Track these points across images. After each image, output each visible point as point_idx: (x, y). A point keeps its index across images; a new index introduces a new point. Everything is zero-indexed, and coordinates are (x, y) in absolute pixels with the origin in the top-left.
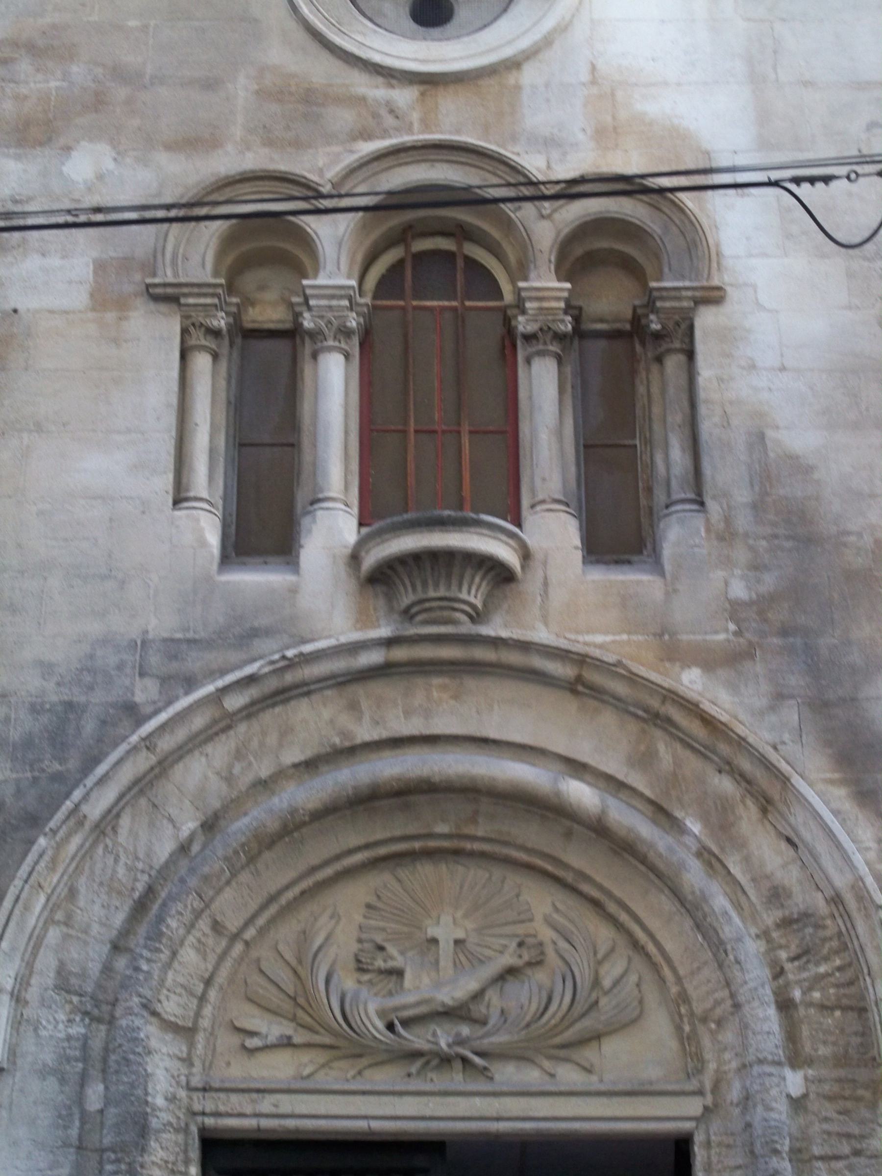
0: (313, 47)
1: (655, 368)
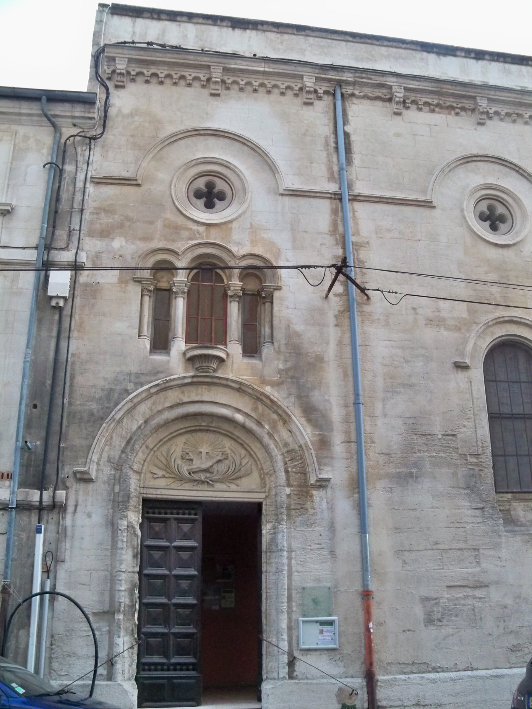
0: (178, 213)
1: (263, 306)
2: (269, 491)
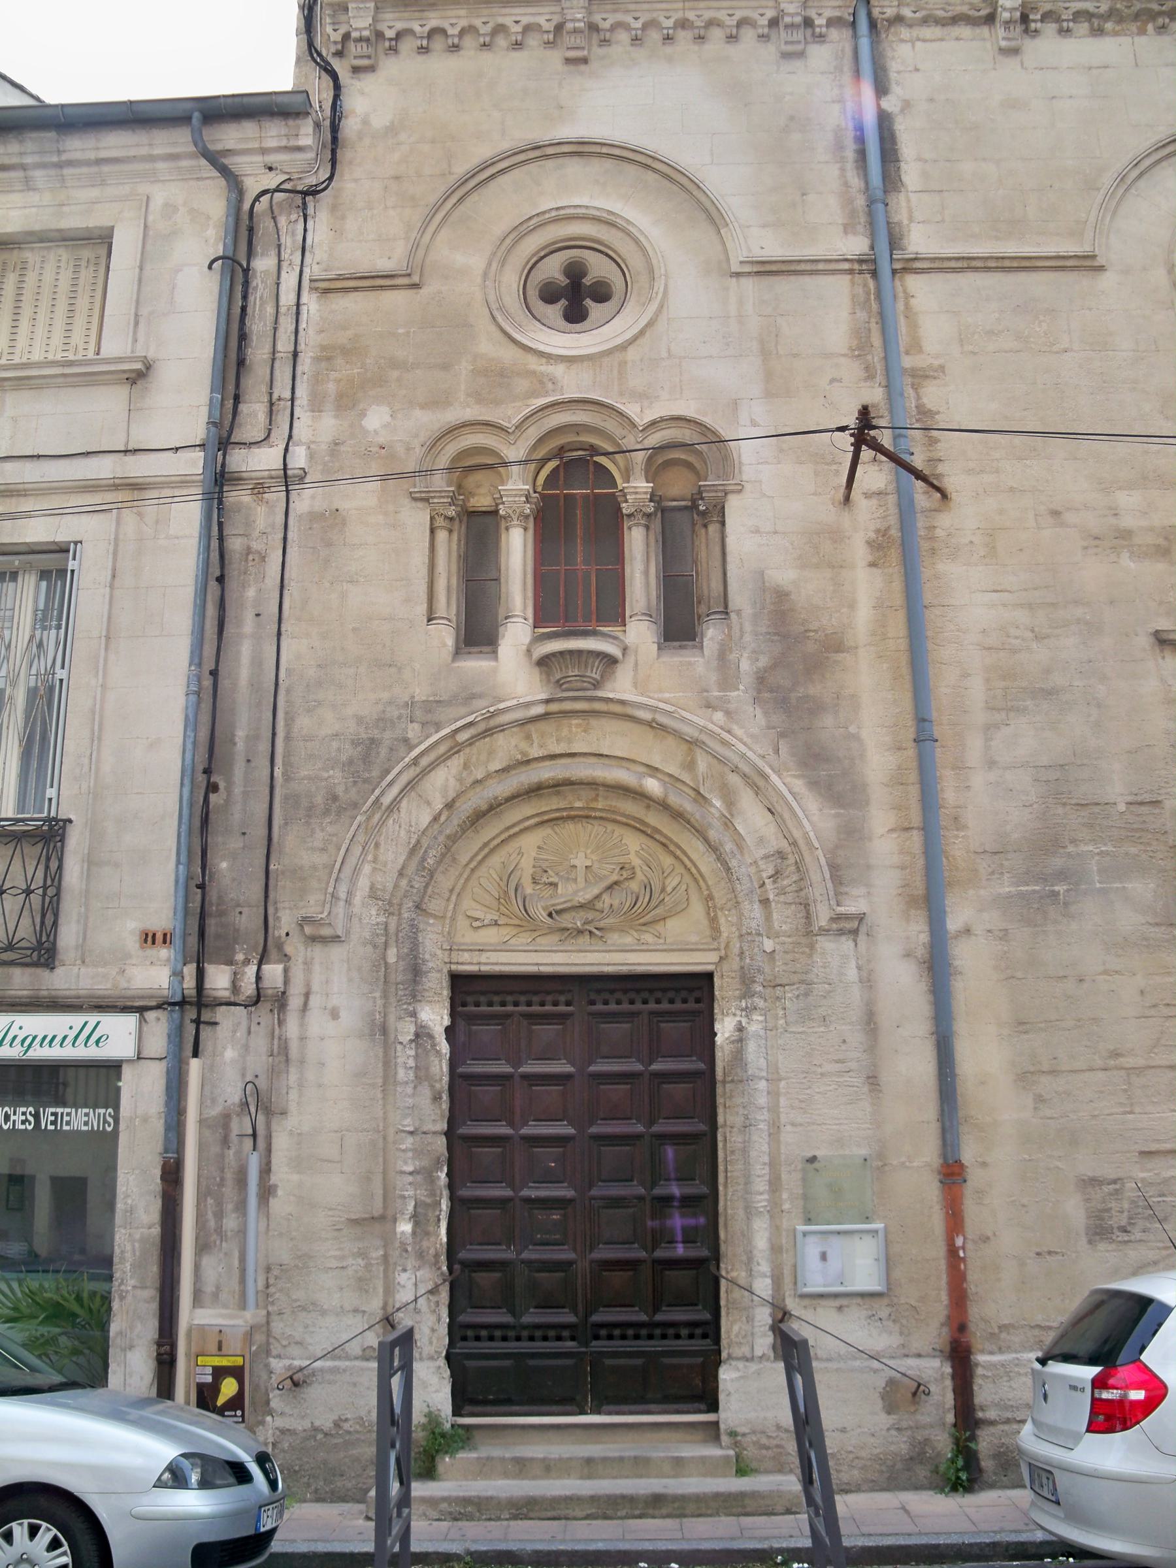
0: (504, 340)
1: (703, 531)
2: (727, 946)
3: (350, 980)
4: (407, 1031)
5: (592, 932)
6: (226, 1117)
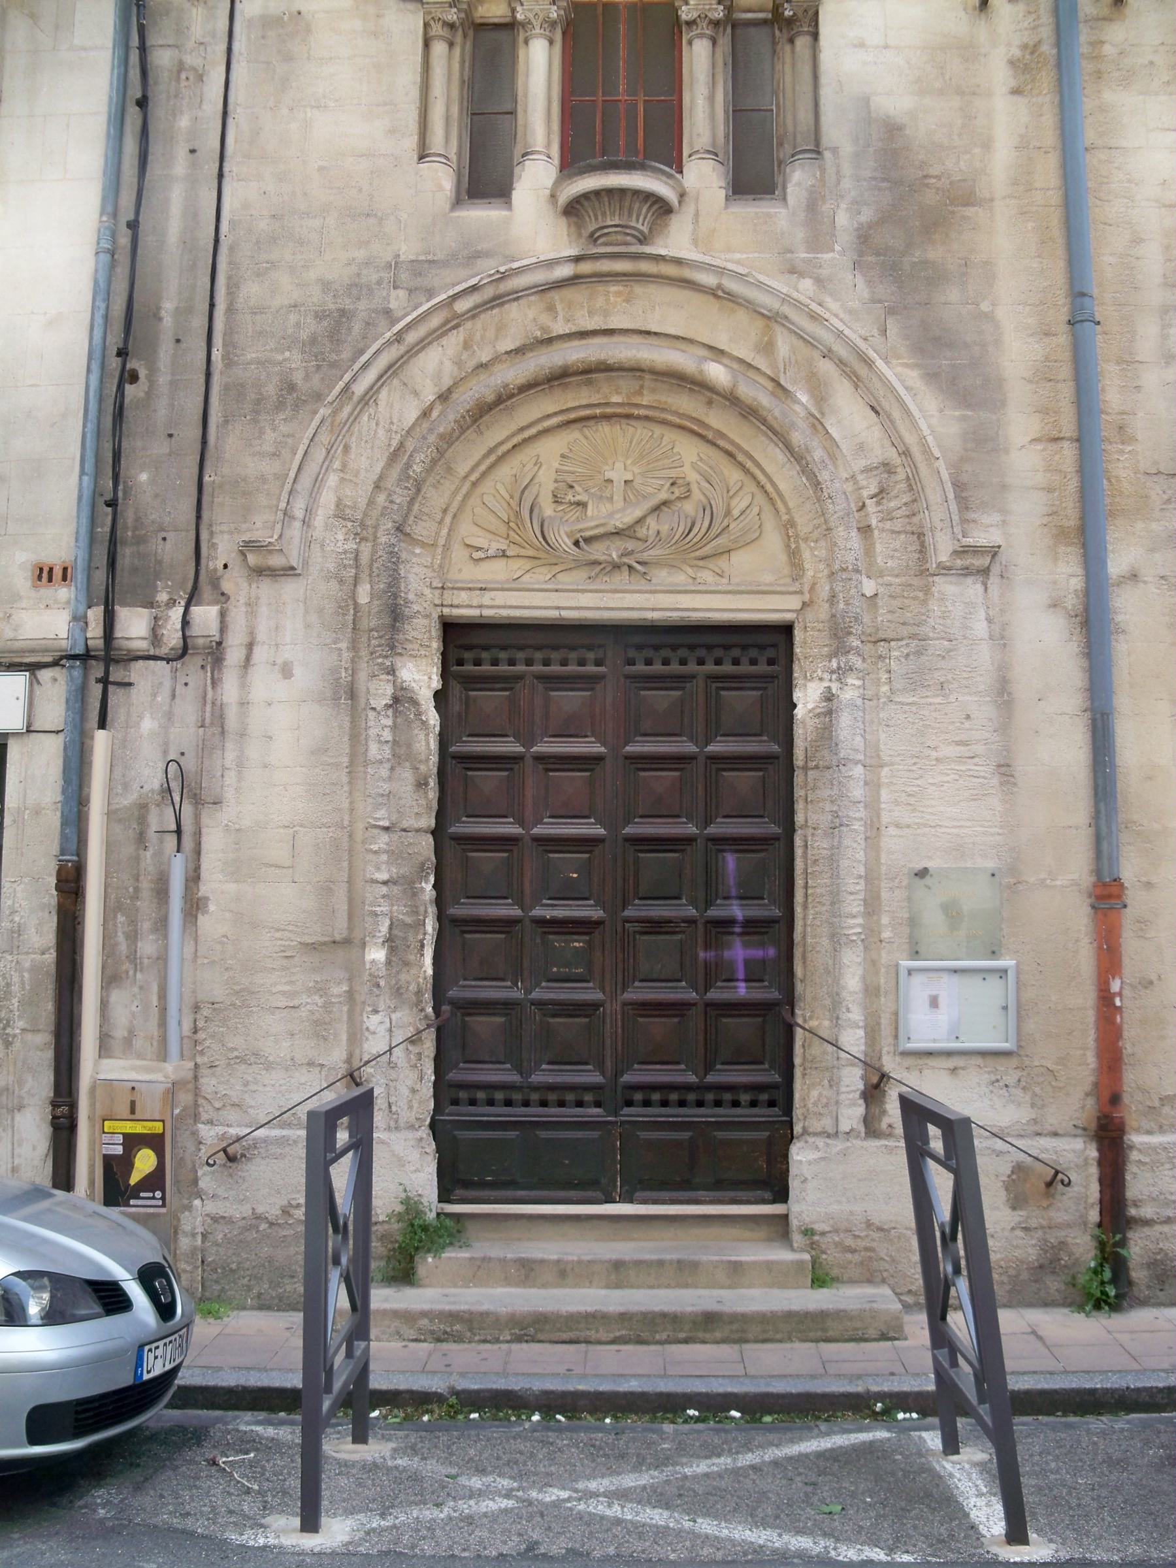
1: (788, 48)
2: (812, 589)
3: (308, 626)
4: (381, 693)
5: (632, 568)
6: (142, 808)
